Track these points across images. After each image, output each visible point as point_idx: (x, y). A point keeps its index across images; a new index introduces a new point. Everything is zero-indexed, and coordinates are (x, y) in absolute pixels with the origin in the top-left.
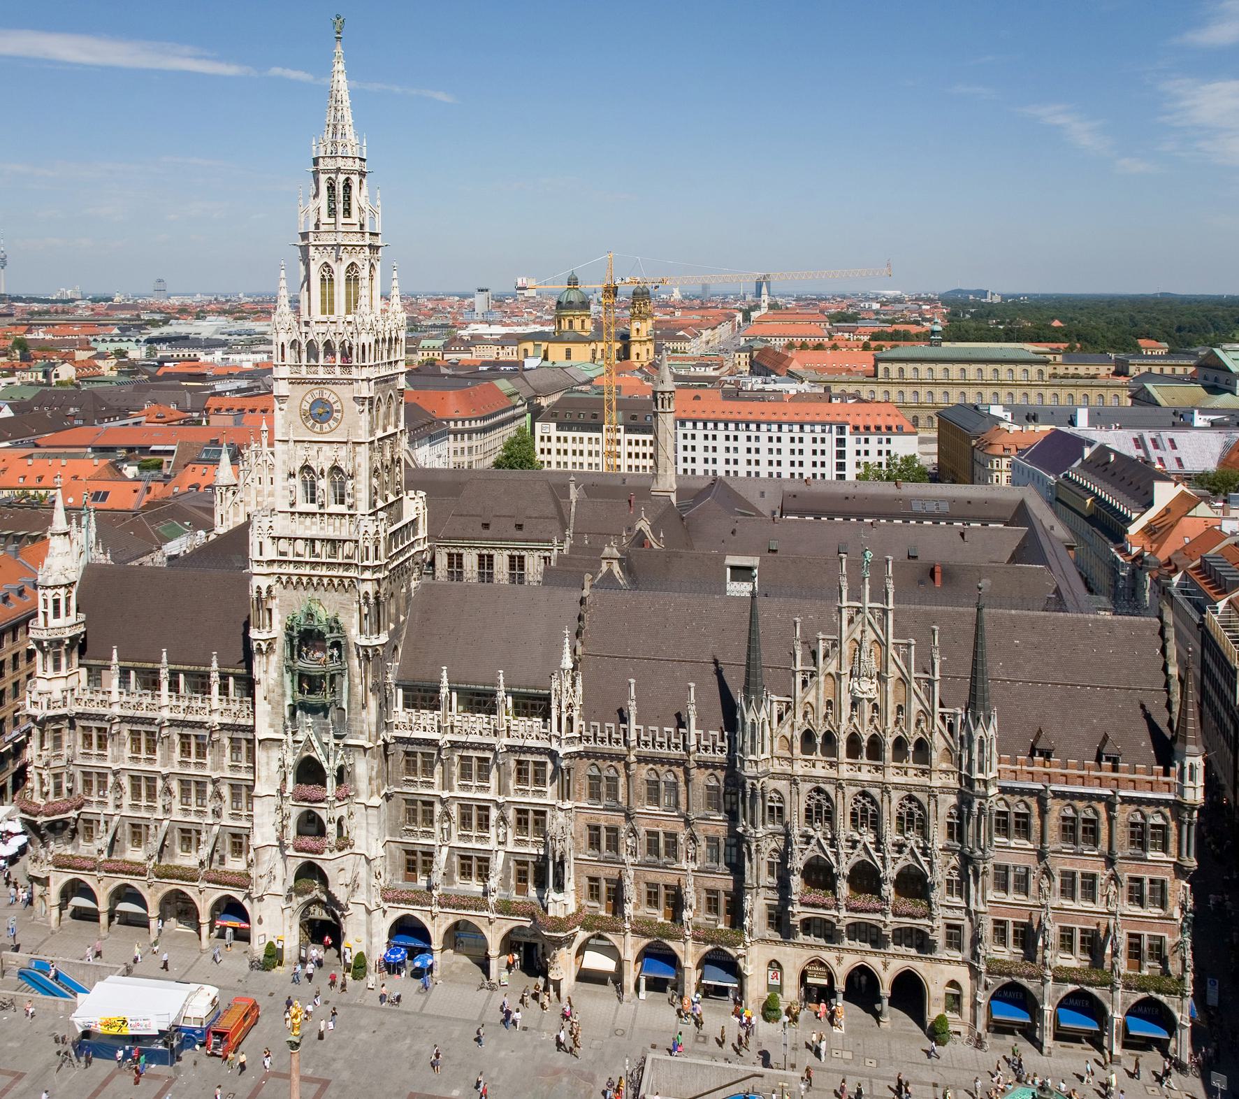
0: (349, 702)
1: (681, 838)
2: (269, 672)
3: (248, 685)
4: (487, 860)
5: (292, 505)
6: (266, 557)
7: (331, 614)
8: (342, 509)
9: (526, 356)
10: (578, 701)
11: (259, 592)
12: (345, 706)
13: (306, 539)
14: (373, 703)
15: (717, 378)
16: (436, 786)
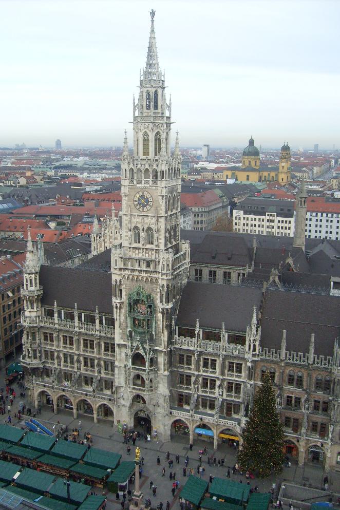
0: (155, 331)
1: (303, 400)
2: (121, 317)
3: (111, 323)
4: (214, 401)
5: (130, 244)
6: (118, 267)
7: (147, 293)
8: (153, 246)
9: (227, 178)
10: (258, 338)
11: (116, 282)
12: (154, 333)
13: (136, 260)
14: (166, 333)
15: (323, 191)
16: (192, 369)
